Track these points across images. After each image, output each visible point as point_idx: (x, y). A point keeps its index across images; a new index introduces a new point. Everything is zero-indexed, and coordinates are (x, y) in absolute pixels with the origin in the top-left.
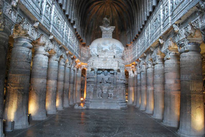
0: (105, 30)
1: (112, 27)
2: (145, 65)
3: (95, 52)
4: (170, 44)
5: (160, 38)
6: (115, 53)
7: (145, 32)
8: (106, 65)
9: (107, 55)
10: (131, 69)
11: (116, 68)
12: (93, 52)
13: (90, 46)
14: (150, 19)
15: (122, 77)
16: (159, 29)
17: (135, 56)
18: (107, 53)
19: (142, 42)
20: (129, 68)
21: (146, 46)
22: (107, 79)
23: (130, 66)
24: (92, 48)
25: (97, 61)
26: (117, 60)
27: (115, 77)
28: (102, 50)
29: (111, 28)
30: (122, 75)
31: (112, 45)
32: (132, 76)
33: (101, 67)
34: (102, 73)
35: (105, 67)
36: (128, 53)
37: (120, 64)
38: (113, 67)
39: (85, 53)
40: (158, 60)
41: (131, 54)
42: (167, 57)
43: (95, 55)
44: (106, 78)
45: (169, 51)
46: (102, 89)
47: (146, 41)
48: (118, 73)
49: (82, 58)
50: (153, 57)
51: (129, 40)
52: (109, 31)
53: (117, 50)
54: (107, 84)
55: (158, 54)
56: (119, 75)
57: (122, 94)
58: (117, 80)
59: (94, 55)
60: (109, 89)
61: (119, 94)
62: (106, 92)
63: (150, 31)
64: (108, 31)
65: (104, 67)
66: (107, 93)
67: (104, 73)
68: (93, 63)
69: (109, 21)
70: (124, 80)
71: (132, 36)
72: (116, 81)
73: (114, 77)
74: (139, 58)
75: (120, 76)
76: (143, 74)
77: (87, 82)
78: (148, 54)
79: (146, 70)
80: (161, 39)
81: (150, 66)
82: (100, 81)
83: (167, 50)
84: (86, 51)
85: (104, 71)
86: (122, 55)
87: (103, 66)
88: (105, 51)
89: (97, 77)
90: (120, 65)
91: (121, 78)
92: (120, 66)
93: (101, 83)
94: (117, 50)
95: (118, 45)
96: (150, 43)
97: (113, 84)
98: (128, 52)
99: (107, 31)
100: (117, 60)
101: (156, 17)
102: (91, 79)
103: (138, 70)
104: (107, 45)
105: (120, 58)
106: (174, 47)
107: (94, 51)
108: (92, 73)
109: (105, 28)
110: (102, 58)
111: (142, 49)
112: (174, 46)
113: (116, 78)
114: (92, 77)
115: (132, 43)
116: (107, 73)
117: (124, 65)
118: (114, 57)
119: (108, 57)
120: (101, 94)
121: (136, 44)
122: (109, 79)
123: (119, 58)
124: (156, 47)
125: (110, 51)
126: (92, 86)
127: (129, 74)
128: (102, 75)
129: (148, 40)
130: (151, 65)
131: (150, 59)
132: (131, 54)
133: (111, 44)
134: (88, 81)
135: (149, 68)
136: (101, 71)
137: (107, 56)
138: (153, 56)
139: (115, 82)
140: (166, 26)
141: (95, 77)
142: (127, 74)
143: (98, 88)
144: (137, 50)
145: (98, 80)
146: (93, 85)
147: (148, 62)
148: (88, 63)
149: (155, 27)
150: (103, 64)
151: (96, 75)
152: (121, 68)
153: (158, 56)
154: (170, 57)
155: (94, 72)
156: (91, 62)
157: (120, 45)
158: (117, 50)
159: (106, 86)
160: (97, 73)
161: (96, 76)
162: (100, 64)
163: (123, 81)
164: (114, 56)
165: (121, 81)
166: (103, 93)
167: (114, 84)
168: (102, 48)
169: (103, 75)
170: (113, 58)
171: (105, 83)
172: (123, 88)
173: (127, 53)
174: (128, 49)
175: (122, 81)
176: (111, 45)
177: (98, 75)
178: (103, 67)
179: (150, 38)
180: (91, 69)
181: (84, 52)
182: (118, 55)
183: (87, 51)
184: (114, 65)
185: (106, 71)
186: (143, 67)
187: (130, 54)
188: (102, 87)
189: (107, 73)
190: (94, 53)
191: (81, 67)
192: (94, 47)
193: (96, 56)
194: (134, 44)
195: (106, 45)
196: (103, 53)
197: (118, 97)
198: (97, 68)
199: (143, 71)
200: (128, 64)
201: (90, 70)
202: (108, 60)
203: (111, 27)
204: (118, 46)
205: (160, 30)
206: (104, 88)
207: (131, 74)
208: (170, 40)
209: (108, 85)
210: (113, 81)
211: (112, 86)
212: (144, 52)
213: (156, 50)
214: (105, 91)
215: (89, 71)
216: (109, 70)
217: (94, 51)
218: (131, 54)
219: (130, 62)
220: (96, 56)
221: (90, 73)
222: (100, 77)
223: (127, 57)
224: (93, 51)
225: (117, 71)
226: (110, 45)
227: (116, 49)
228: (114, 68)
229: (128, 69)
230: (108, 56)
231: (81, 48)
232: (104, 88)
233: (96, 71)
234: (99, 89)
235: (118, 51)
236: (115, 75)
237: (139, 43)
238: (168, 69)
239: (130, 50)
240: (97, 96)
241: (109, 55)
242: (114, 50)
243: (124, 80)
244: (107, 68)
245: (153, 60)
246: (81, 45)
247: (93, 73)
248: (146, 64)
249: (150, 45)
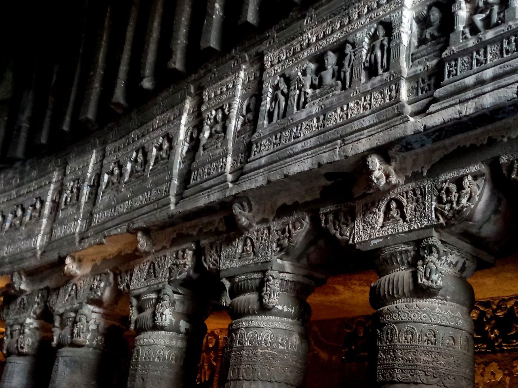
2: (97, 310)
4: (477, 199)
5: (384, 152)
7: (169, 115)
14: (261, 42)
16: (377, 100)
17: (24, 245)
19: (129, 166)
21: (173, 191)
40: (277, 288)
42: (422, 281)
45: (439, 244)
47: (178, 165)
50: (236, 264)
55: (287, 254)
63: (234, 112)
74: (68, 261)
76: (74, 363)
78: (174, 242)
79: (94, 343)
80: (387, 159)
81: (167, 316)
83: (435, 234)
96: (230, 177)
101: (338, 35)
103: (26, 330)
106: (481, 228)
111: (108, 207)
112: (488, 220)
115: (18, 164)
121: (56, 174)
124: (283, 211)
129: (216, 160)
130: (174, 313)
131: (184, 275)
135: (162, 328)
138: (230, 258)
140: (481, 82)
144: (46, 211)
147: (158, 292)
149: (310, 91)
153: (283, 266)
154: (440, 283)
179: (246, 150)
186: (84, 320)
194: (34, 174)
199: (80, 346)
205: (376, 105)
208: (475, 177)
212: (139, 223)
213: (275, 226)
237: (89, 175)
238: (423, 357)
245: (227, 284)
248: (134, 302)
249: (232, 190)
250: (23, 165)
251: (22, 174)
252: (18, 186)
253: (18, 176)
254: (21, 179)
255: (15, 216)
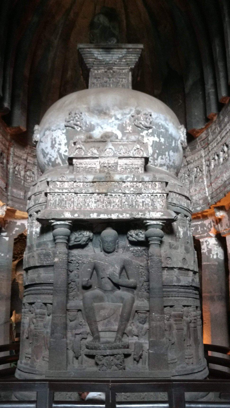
0: (101, 63)
1: (130, 46)
3: (59, 149)
6: (150, 150)
8: (110, 203)
9: (113, 156)
10: (212, 229)
11: (158, 215)
12: (49, 150)
13: (36, 127)
15: (188, 256)
18: (110, 146)
20: (203, 226)
22: (118, 268)
23: (205, 217)
24: (44, 135)
25: (66, 185)
26: (158, 176)
27: (155, 258)
28: (90, 137)
29: (124, 51)
30: (187, 250)
31: (133, 112)
32: (215, 257)
33: (84, 213)
34: (90, 244)
35: (106, 212)
36: (195, 164)
37: (174, 198)
38: (141, 211)
39: (28, 173)
41: (212, 166)
43: (59, 161)
44: (111, 265)
46: (95, 321)
48: (167, 239)
49: (12, 192)
51: (197, 113)
52: (120, 65)
53: (156, 139)
54: (119, 292)
56: (171, 246)
57: (191, 341)
58: (165, 272)
59: (55, 164)
60: (128, 320)
61: (175, 340)
62: (114, 335)
64: (114, 64)
65: (99, 213)
66: (120, 340)
67: (103, 241)
68: (46, 194)
69: (116, 32)
70: (195, 273)
71: (210, 90)
72: (161, 276)
73: (149, 257)
75: (174, 252)
77: (26, 287)
82: (85, 279)
84: (29, 167)
85: (99, 233)
86: (177, 163)
87: (93, 206)
88: (105, 139)
89: (69, 262)
90: (175, 202)
91: (180, 265)
92: (176, 209)
93: (87, 288)
94: (159, 137)
95: (162, 116)
97: (145, 293)
98: (195, 161)
99: (109, 66)
100: (158, 176)
102: (41, 270)
104: (112, 113)
105: (171, 176)
107: (53, 147)
108: (45, 243)
109: (98, 54)
110: (89, 171)
113: (161, 262)
114: (45, 264)
115: (215, 118)
116: (115, 242)
117: (188, 206)
118: (146, 169)
119: (117, 163)
120: (87, 347)
122: (123, 268)
123: (166, 173)
125: (127, 138)
126: (45, 304)
127: (204, 249)
128: (93, 253)
132: (209, 166)
133: (127, 111)
134: (27, 284)
136: (87, 234)
137: (112, 161)
139: (154, 284)
141: (56, 260)
142: (197, 245)
143: (71, 313)
145: (72, 274)
146: (48, 299)
148: (29, 199)
150: (93, 200)
151: (62, 249)
152: (179, 217)
155: (54, 240)
156: (40, 193)
157: (168, 117)
158: (156, 139)
159: (113, 302)
160: (69, 240)
161: (65, 257)
162: (80, 198)
163: (189, 279)
164: (147, 160)
165: (181, 278)
166: (97, 338)
167: (149, 290)
168: (92, 128)
169: (98, 251)
170: (141, 171)
171: (105, 291)
172: (191, 309)
173: (192, 166)
174: (193, 149)
175: (187, 275)
176: (129, 115)
177: (75, 252)
178: (93, 212)
180: (40, 226)
181: (21, 167)
182: (159, 161)
183: (34, 164)
184: (148, 201)
185: (109, 233)
187: (205, 168)
188: (92, 309)
189: (115, 242)
190: (53, 154)
191: (9, 230)
192: (53, 128)
193: (62, 165)
195: (105, 114)
196: (94, 147)
197: (172, 355)
198: (68, 215)
200: (199, 209)
201: (37, 228)
202: (117, 177)
203: (123, 46)
204: (163, 122)
206: (103, 313)
207: (210, 251)
209: (122, 299)
210: (145, 278)
211: (141, 303)
214: (109, 327)
215: (35, 236)
216: (123, 227)
217: (53, 147)
218: (212, 166)
219: (205, 199)
220: (62, 168)
221: (35, 243)
222: (85, 260)
223: (191, 182)
224: (49, 145)
225: (162, 229)
226: (124, 114)
227: (150, 131)
228: (147, 216)
229: (197, 229)
230: (116, 160)
231: (8, 149)
232: (103, 313)
233: (62, 230)
234: (81, 319)
235: (162, 140)
236: (154, 249)
239: (203, 153)
240: (71, 354)
241: (122, 155)
242: (143, 137)
243: (195, 273)
244: (114, 217)
246: (9, 137)
247: (50, 245)
250: (219, 117)
251: (220, 124)
252: (220, 132)
253: (218, 126)
254: (220, 126)
255: (224, 152)
